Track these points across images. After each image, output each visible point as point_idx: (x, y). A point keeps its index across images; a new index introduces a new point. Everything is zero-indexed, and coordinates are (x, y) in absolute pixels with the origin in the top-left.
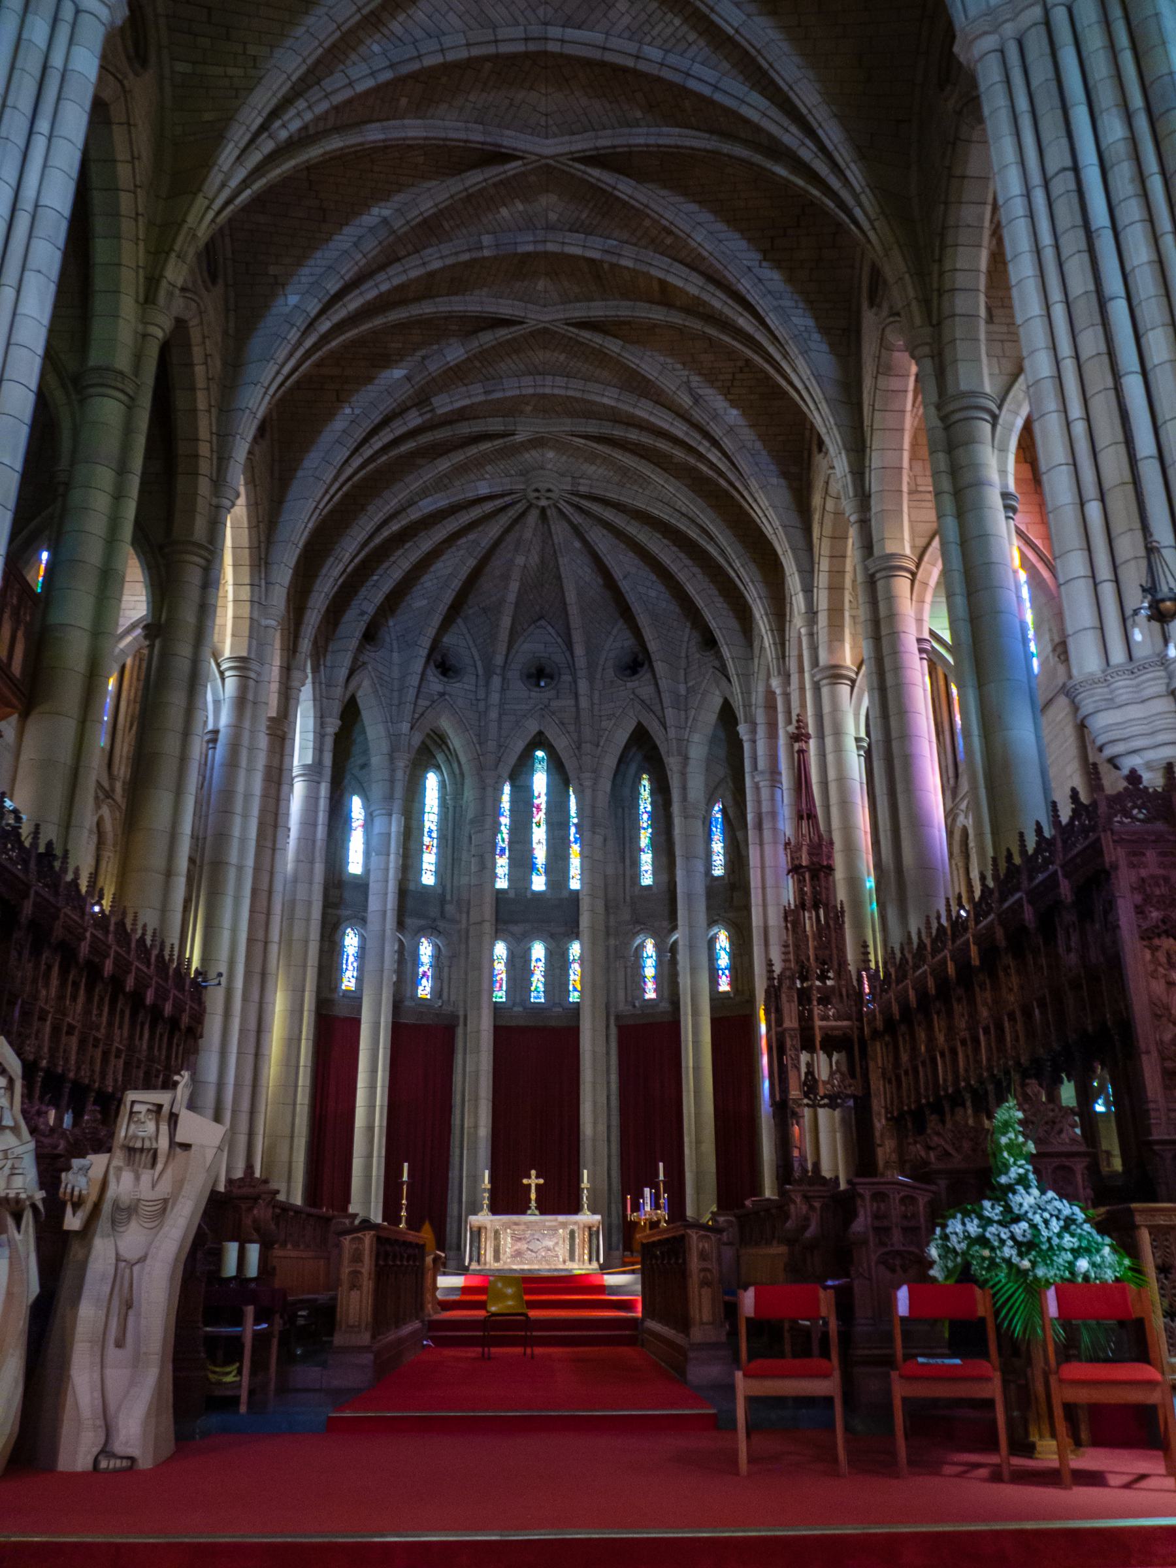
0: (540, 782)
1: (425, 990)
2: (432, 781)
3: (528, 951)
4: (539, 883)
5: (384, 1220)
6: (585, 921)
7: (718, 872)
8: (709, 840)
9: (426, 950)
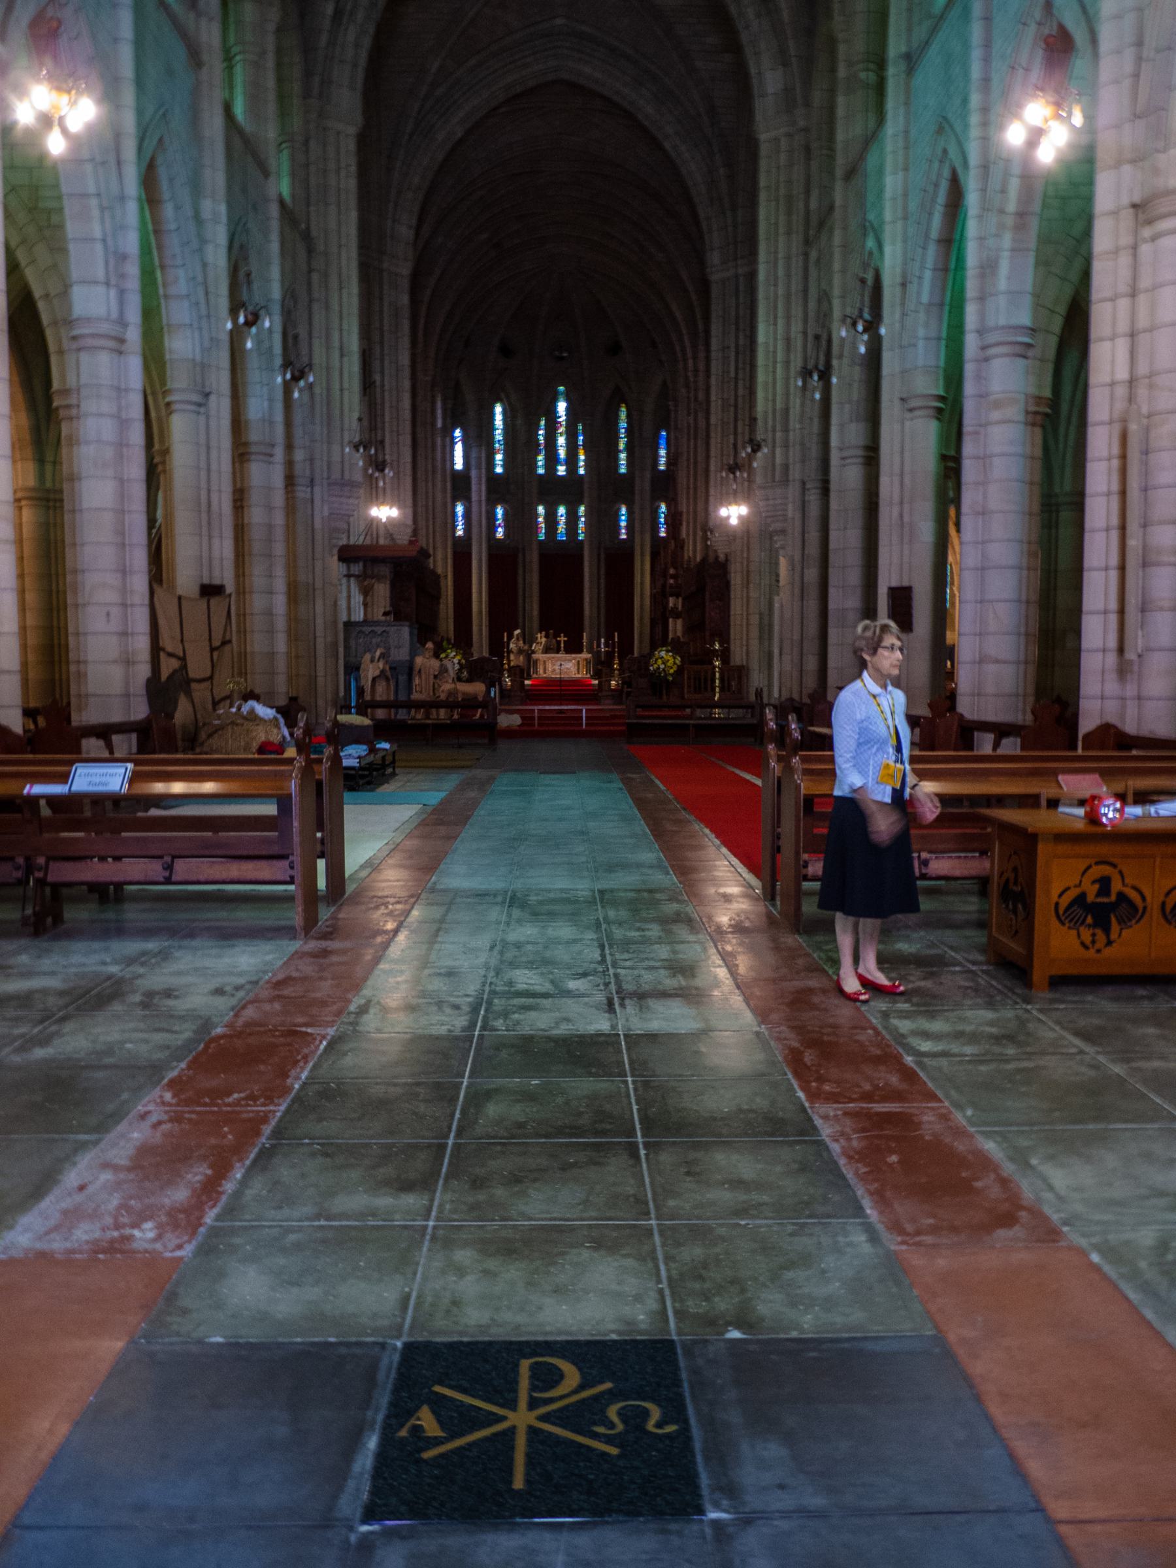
0: (562, 407)
1: (500, 533)
2: (498, 409)
3: (555, 513)
4: (561, 470)
5: (491, 653)
6: (586, 494)
7: (662, 468)
8: (656, 448)
9: (500, 511)
